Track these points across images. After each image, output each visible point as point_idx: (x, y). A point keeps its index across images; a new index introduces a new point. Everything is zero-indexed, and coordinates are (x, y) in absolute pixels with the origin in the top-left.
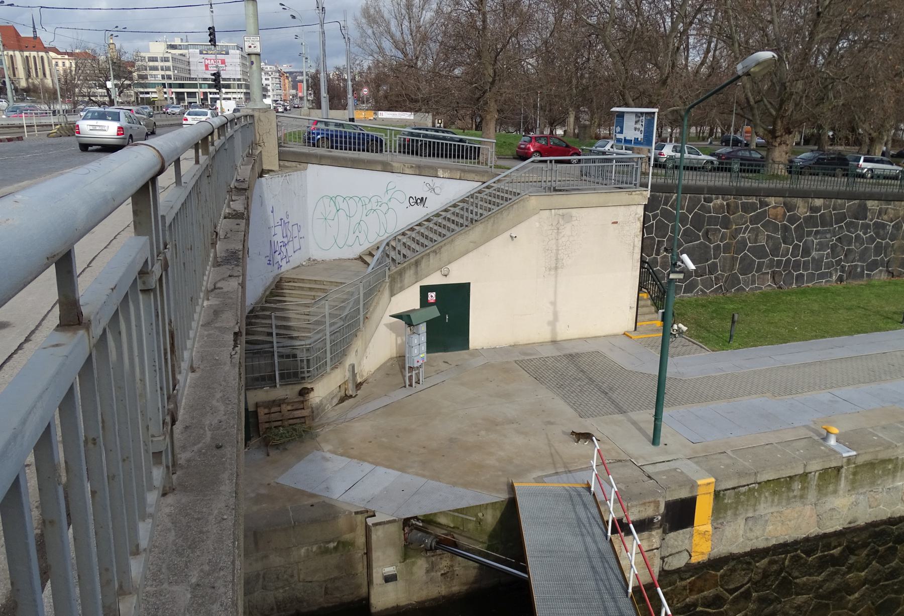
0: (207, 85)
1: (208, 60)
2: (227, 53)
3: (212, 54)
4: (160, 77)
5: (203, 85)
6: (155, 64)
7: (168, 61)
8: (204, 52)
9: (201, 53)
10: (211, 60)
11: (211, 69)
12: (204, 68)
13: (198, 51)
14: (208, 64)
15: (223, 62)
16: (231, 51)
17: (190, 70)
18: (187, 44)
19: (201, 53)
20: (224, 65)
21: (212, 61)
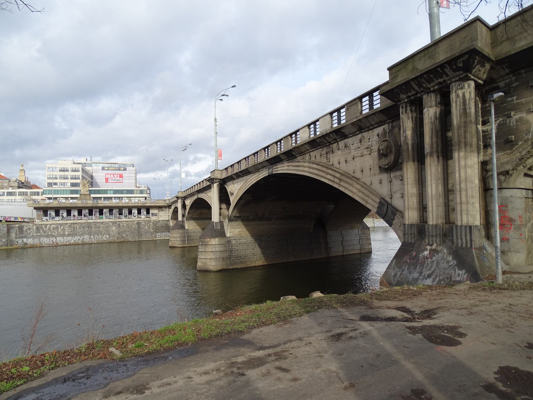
0: (112, 191)
1: (108, 174)
2: (125, 170)
3: (112, 170)
4: (69, 184)
5: (109, 192)
6: (66, 173)
7: (78, 171)
8: (106, 169)
9: (103, 169)
10: (111, 174)
11: (111, 181)
12: (104, 181)
13: (101, 168)
14: (108, 178)
15: (121, 176)
16: (128, 168)
17: (92, 183)
18: (91, 162)
19: (103, 169)
20: (122, 179)
21: (112, 175)
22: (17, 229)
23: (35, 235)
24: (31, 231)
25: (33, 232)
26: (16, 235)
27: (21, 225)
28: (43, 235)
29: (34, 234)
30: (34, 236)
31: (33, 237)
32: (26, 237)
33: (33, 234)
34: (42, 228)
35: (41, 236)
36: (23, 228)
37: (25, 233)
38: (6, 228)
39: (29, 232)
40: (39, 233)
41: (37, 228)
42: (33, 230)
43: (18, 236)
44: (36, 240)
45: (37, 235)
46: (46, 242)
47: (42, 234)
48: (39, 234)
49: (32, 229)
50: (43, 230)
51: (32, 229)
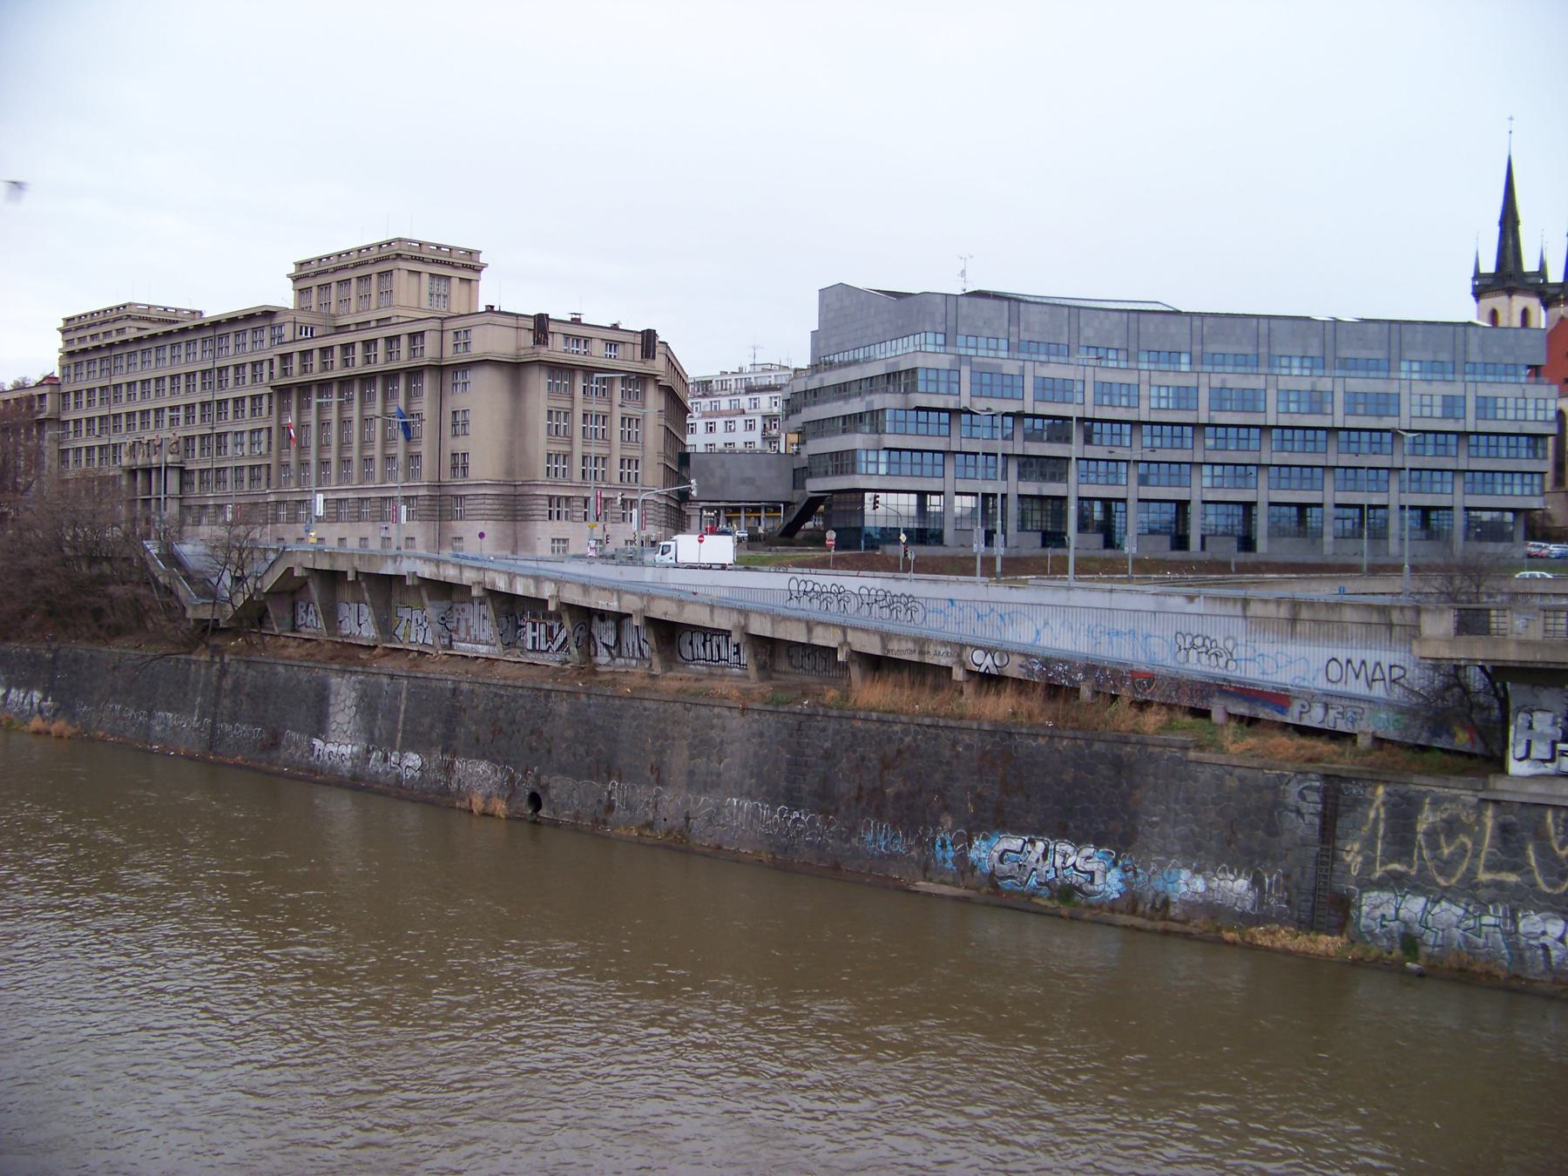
22: (1376, 819)
23: (1487, 886)
24: (1463, 845)
25: (1476, 855)
26: (1369, 863)
27: (1402, 789)
28: (1541, 895)
29: (1484, 877)
30: (1476, 886)
31: (1468, 891)
32: (1419, 885)
33: (1472, 872)
34: (1540, 836)
35: (1519, 900)
36: (1419, 810)
37: (1421, 857)
38: (1315, 797)
39: (1446, 851)
40: (1514, 868)
41: (1504, 830)
42: (1478, 842)
43: (1378, 872)
44: (1487, 920)
45: (1500, 885)
46: (1554, 953)
47: (1534, 885)
48: (1512, 878)
49: (1466, 829)
50: (1545, 852)
51: (1466, 829)
